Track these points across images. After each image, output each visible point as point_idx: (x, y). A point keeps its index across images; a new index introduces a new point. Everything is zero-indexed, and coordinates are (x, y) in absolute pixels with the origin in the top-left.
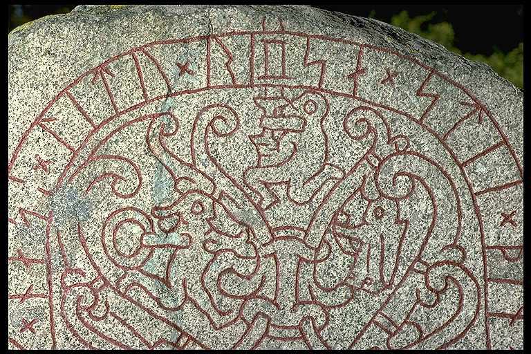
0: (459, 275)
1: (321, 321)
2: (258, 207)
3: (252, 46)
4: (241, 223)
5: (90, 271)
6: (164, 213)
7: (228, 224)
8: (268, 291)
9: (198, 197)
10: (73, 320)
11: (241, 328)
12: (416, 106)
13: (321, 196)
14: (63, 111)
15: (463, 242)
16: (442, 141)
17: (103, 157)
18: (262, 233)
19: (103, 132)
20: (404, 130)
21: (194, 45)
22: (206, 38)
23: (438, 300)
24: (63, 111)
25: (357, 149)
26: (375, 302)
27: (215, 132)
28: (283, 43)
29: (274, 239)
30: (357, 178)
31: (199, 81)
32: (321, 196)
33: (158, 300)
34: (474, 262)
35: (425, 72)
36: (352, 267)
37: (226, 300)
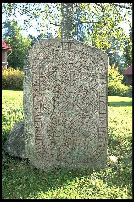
0: (96, 77)
1: (76, 83)
2: (68, 67)
3: (69, 44)
4: (66, 69)
5: (45, 74)
6: (56, 67)
7: (64, 69)
8: (69, 79)
10: (43, 82)
11: (65, 84)
12: (91, 54)
13: (77, 65)
14: (42, 52)
15: (96, 73)
16: (94, 59)
17: (48, 59)
18: (69, 70)
19: (48, 55)
21: (61, 44)
22: (62, 43)
23: (93, 81)
24: (42, 52)
25: (82, 59)
26: (84, 81)
27: (63, 56)
29: (70, 71)
30: (82, 63)
31: (61, 49)
32: (77, 65)
33: (54, 79)
35: (92, 49)
36: (81, 76)
37: (64, 80)
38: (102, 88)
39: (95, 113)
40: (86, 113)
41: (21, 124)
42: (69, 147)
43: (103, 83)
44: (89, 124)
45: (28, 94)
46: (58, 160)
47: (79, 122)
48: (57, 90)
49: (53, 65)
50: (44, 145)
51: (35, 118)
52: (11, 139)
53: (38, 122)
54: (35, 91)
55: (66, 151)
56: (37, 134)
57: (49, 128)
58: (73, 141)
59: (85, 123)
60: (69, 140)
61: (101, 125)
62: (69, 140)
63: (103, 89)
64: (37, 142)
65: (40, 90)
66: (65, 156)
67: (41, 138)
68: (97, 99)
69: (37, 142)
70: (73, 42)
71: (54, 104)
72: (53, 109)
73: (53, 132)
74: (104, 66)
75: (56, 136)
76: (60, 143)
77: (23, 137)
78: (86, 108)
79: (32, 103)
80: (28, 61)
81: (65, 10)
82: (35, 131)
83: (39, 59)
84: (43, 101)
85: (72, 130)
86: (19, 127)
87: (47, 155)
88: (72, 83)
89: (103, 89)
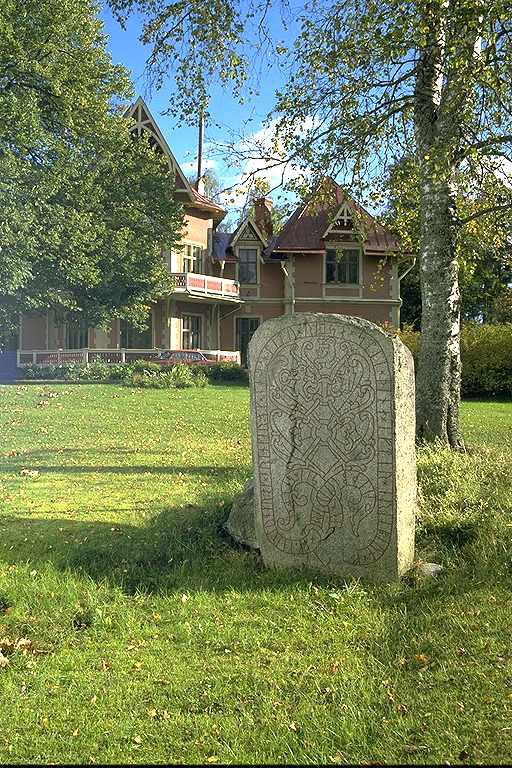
22: (305, 324)
24: (271, 344)
34: (373, 385)
47: (340, 478)
48: (298, 414)
57: (285, 489)
61: (382, 488)
71: (293, 440)
76: (305, 520)
89: (385, 413)
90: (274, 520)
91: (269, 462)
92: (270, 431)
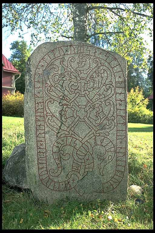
2: (78, 74)
4: (75, 77)
5: (49, 84)
8: (79, 88)
9: (68, 72)
10: (47, 93)
13: (89, 72)
14: (46, 57)
18: (79, 78)
20: (103, 62)
21: (69, 47)
22: (71, 46)
24: (46, 57)
25: (95, 65)
26: (97, 91)
28: (83, 47)
30: (95, 70)
31: (69, 53)
32: (89, 72)
33: (61, 89)
35: (107, 53)
36: (94, 84)
38: (119, 99)
39: (112, 130)
40: (100, 130)
41: (22, 146)
42: (79, 173)
43: (120, 94)
44: (104, 144)
45: (30, 108)
46: (66, 189)
47: (92, 141)
48: (65, 102)
49: (60, 73)
50: (48, 170)
51: (37, 137)
52: (9, 164)
53: (41, 141)
54: (38, 103)
55: (77, 178)
56: (39, 157)
57: (55, 149)
58: (85, 166)
59: (99, 143)
60: (80, 164)
61: (119, 145)
62: (80, 164)
63: (121, 101)
64: (41, 166)
65: (43, 102)
66: (75, 184)
67: (44, 162)
68: (114, 113)
69: (41, 166)
70: (83, 45)
72: (59, 125)
73: (60, 154)
74: (122, 72)
75: (64, 159)
76: (68, 168)
77: (24, 161)
78: (100, 124)
79: (34, 118)
80: (30, 68)
81: (77, 19)
82: (38, 153)
83: (43, 66)
84: (47, 116)
85: (84, 152)
86: (19, 151)
87: (52, 184)
88: (83, 93)
89: (121, 101)
90: (47, 170)
91: (44, 133)
92: (45, 113)
